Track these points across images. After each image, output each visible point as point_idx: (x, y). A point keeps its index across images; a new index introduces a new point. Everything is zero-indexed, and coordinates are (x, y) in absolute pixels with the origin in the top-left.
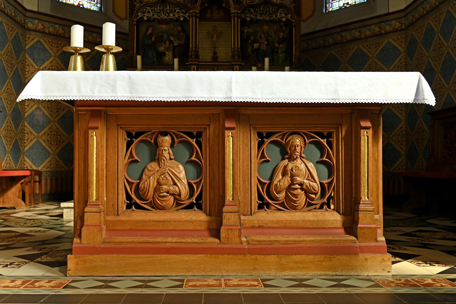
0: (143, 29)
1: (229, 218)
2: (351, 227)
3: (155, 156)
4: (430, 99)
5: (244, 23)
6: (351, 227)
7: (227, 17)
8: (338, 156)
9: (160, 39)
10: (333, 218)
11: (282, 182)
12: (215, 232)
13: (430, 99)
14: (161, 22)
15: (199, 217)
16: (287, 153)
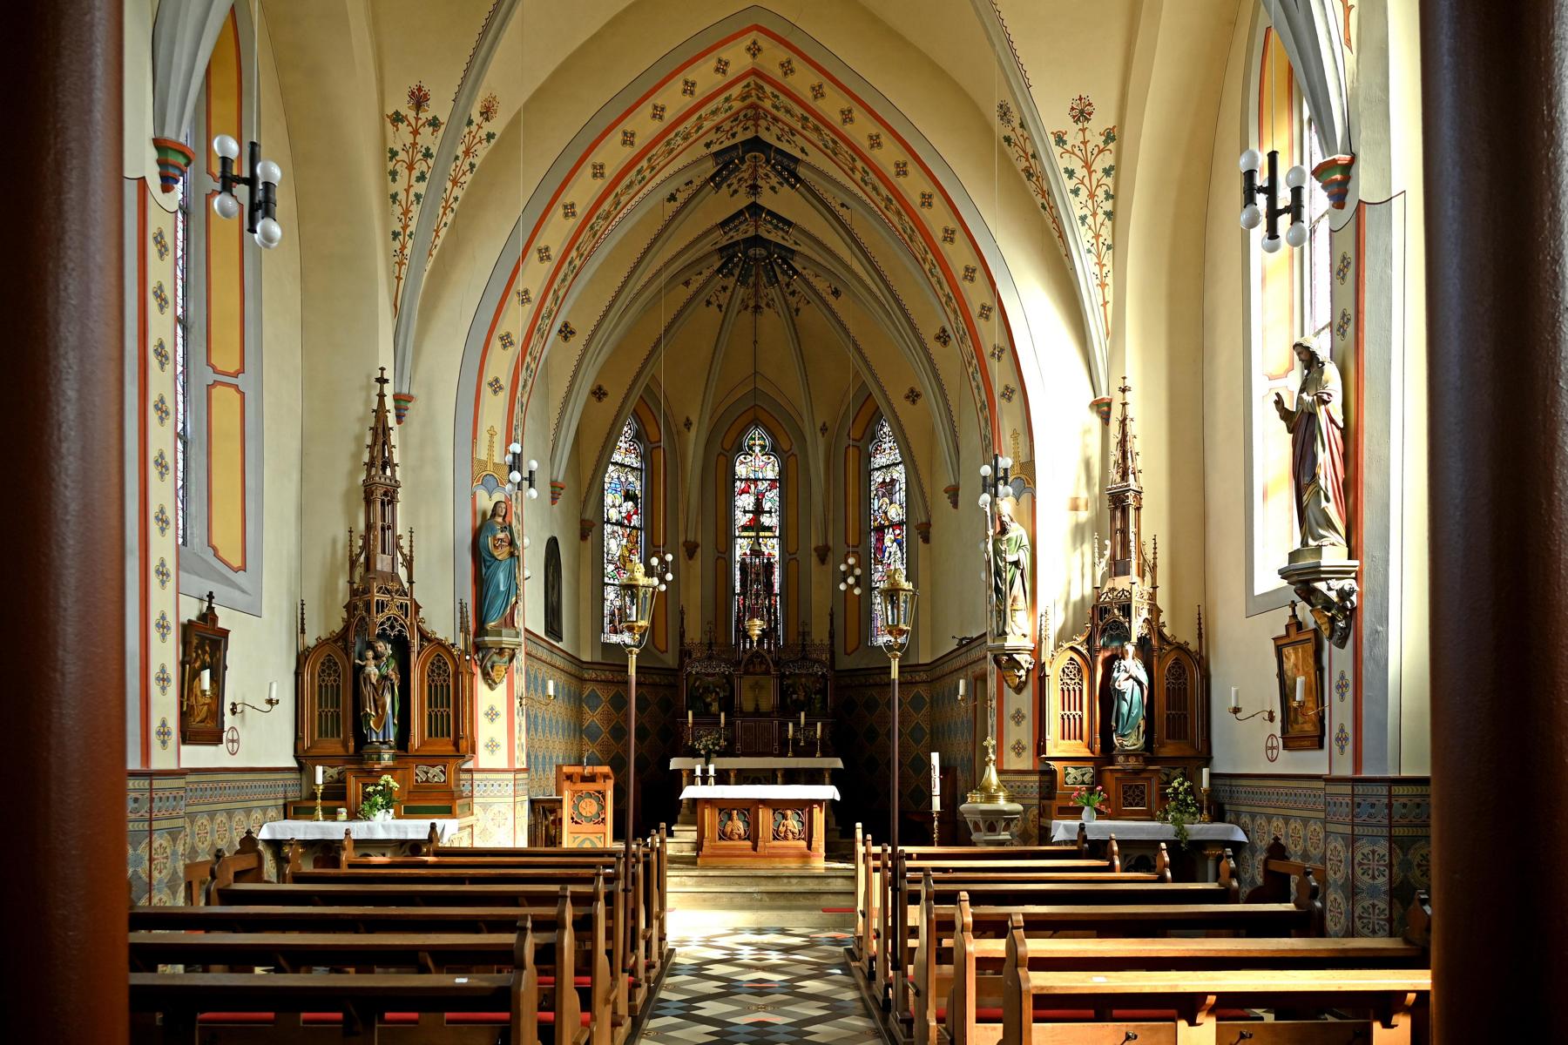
0: (691, 680)
1: (760, 844)
2: (809, 847)
3: (730, 818)
4: (838, 798)
5: (782, 676)
6: (809, 847)
7: (767, 672)
8: (805, 818)
9: (707, 690)
10: (803, 844)
11: (782, 829)
12: (755, 848)
13: (838, 798)
14: (708, 675)
15: (748, 843)
16: (785, 817)
